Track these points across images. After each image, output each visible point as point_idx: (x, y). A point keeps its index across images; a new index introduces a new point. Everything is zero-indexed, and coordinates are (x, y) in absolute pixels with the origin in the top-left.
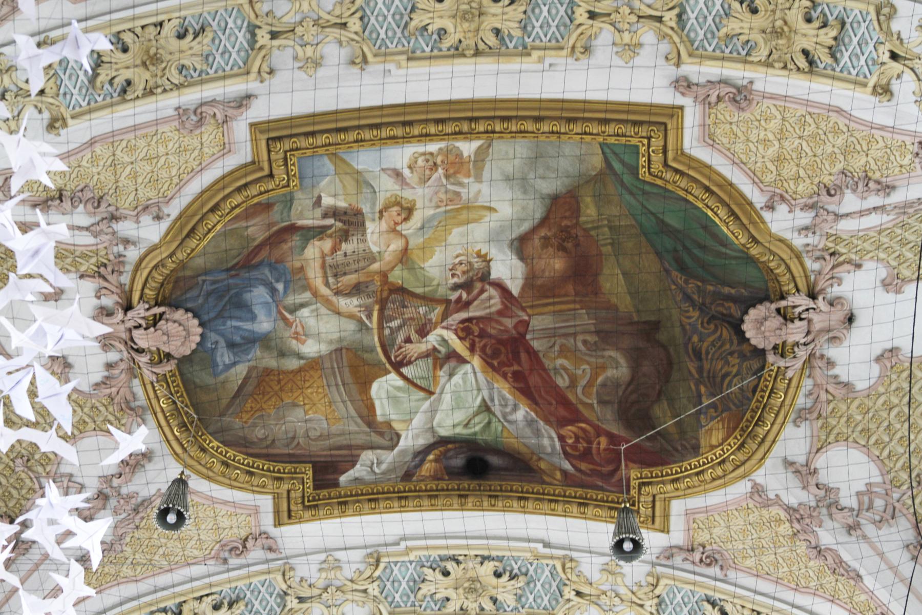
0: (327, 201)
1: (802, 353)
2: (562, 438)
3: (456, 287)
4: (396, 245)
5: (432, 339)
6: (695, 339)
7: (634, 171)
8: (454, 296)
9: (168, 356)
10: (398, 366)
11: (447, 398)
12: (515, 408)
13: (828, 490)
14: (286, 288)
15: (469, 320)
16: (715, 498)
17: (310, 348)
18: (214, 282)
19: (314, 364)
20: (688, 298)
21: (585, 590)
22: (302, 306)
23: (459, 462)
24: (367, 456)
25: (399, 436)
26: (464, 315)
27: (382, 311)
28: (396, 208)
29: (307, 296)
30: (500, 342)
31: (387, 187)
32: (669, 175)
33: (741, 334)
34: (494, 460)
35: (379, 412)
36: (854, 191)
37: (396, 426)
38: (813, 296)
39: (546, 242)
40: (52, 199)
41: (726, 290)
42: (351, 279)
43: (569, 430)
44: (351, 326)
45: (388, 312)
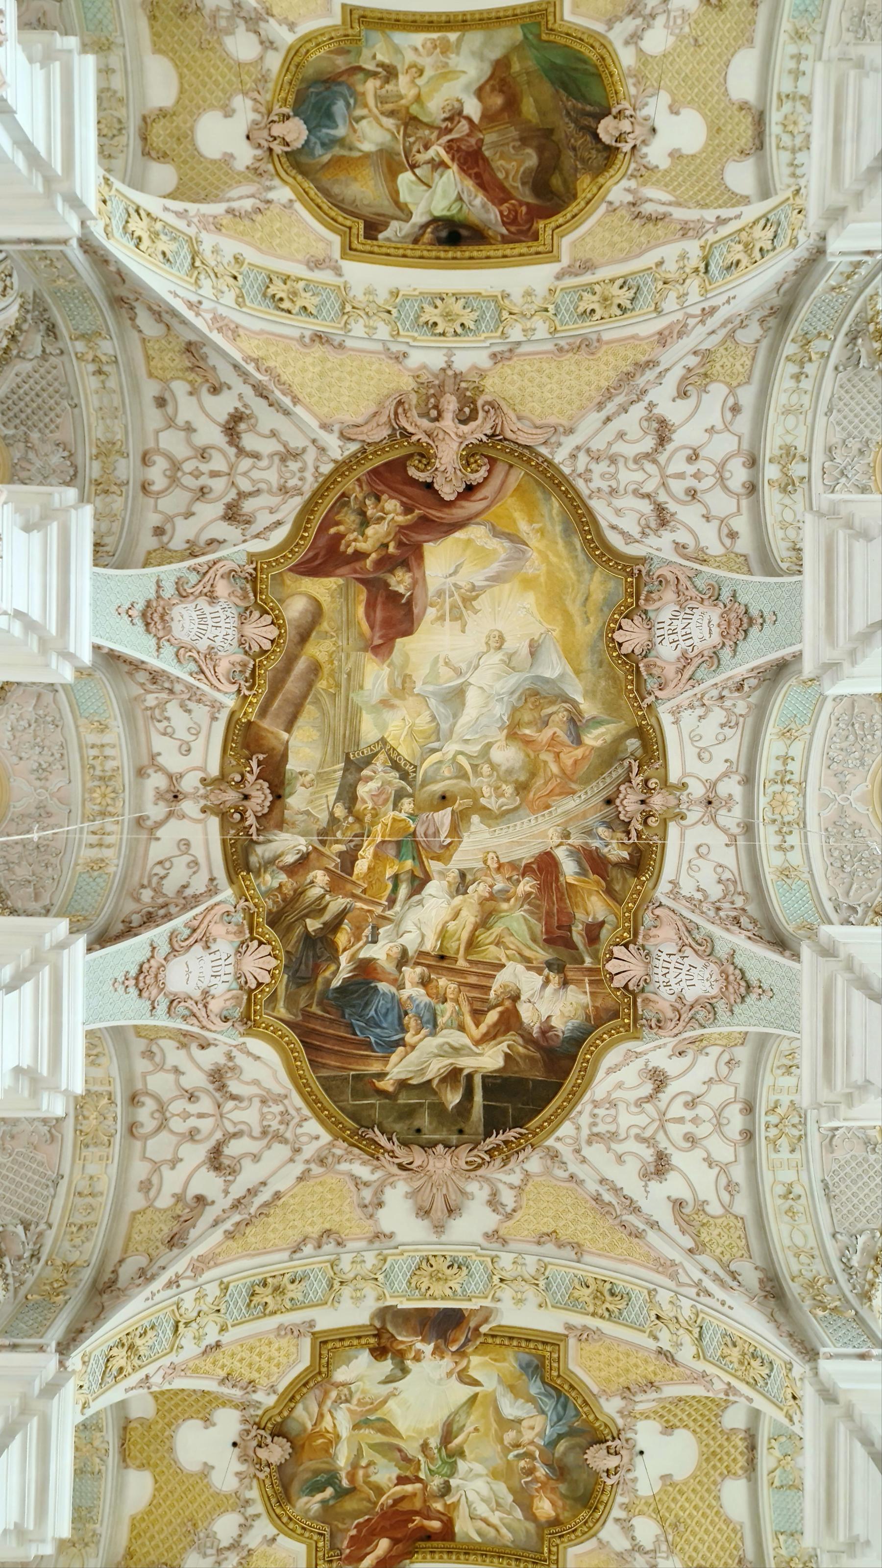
0: (379, 57)
2: (501, 213)
3: (445, 120)
4: (413, 92)
5: (431, 153)
7: (538, 36)
8: (444, 125)
10: (413, 167)
11: (439, 190)
15: (451, 140)
17: (367, 147)
18: (317, 94)
19: (367, 155)
20: (568, 114)
21: (515, 310)
22: (363, 118)
23: (444, 234)
24: (394, 225)
26: (449, 137)
29: (364, 112)
30: (468, 153)
31: (410, 57)
33: (596, 136)
34: (464, 232)
37: (411, 207)
39: (493, 89)
41: (589, 108)
42: (389, 107)
44: (388, 137)
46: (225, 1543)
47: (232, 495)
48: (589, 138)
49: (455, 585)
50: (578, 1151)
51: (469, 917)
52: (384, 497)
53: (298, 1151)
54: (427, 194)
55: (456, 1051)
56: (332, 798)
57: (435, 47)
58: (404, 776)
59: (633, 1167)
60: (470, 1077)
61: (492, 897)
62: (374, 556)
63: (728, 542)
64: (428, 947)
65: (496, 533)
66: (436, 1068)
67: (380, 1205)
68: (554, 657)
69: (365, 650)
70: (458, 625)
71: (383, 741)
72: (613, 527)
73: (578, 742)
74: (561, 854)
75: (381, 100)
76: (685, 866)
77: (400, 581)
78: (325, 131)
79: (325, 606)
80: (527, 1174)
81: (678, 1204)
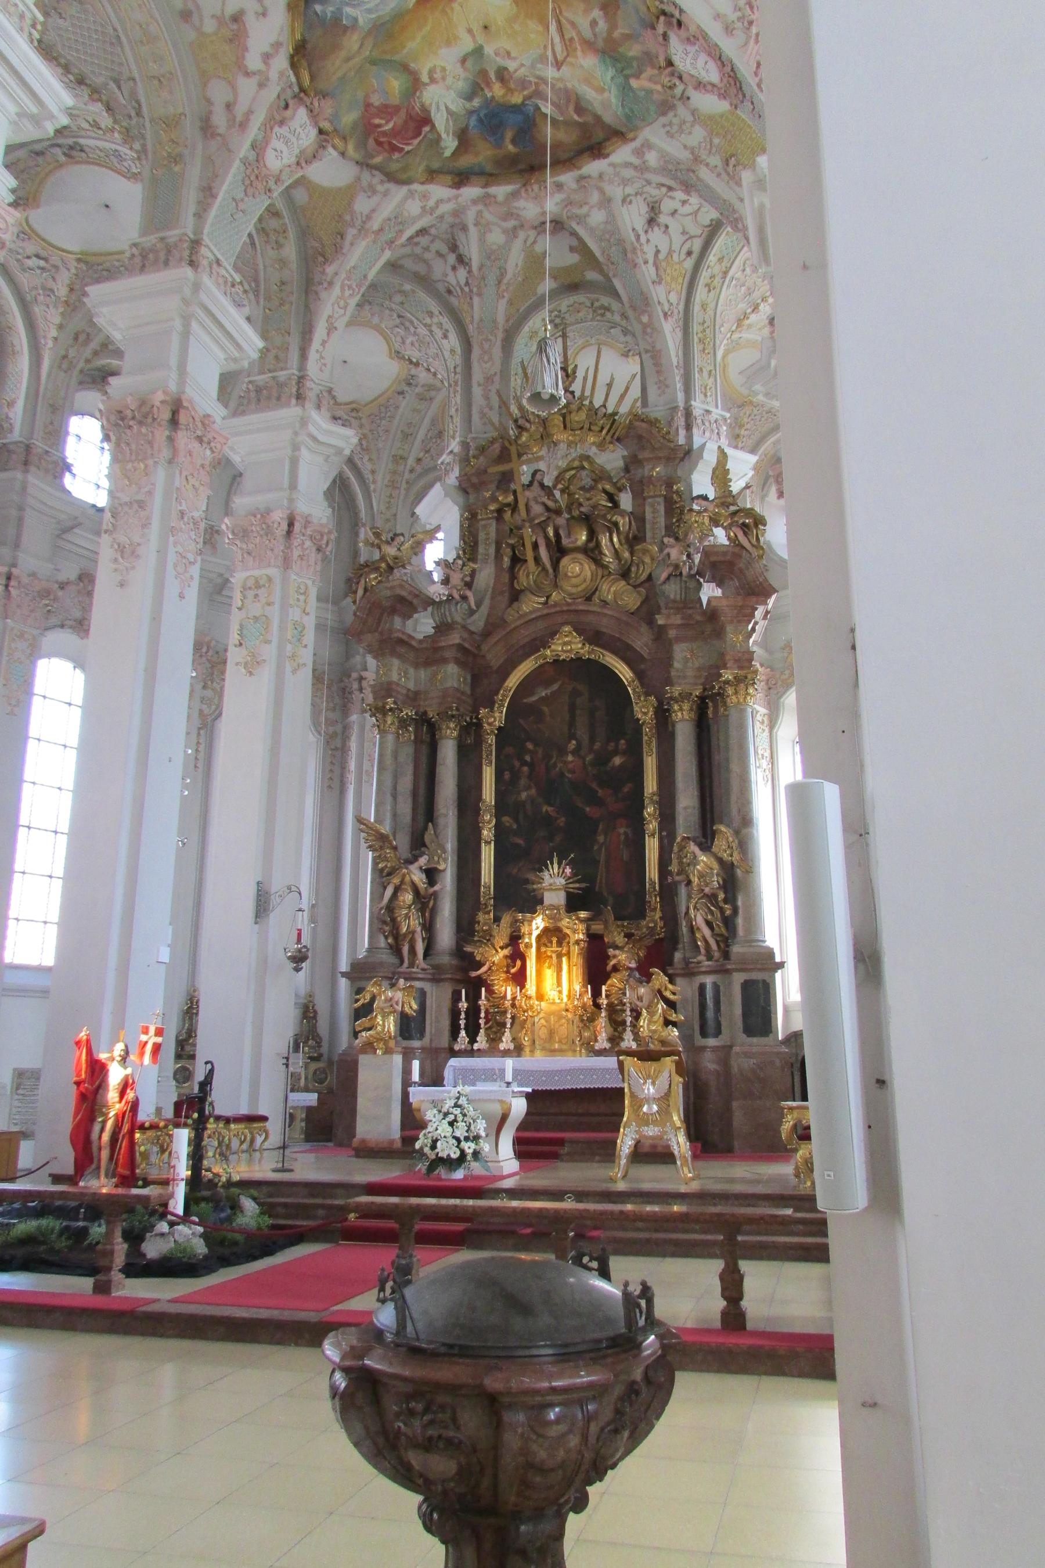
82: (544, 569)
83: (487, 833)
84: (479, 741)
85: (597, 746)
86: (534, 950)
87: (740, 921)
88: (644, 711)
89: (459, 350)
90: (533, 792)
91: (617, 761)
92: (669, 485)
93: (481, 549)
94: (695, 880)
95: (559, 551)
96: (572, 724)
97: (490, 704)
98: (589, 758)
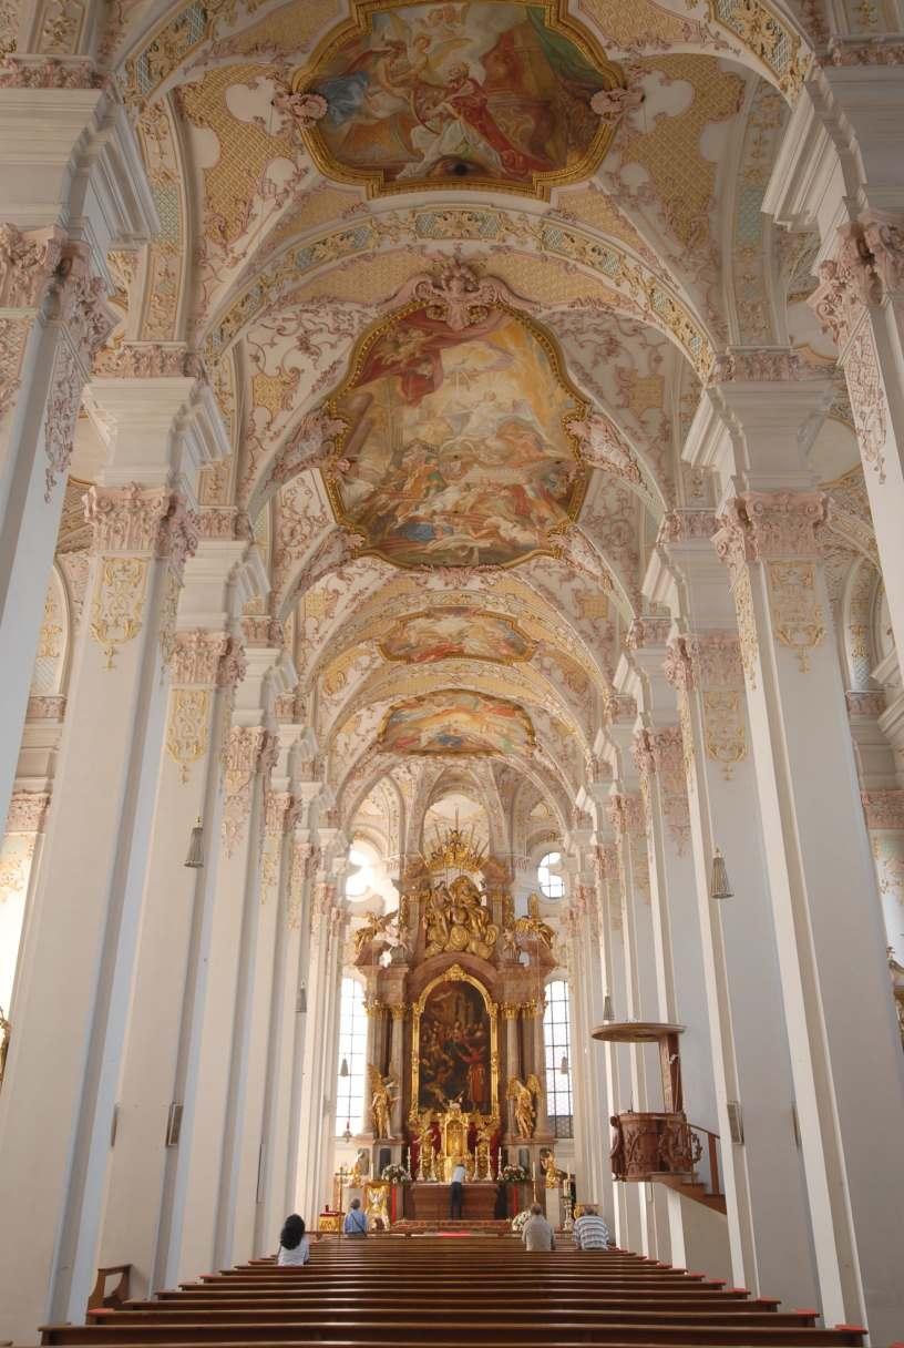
0: (386, 37)
1: (618, 118)
2: (501, 157)
4: (422, 61)
5: (440, 108)
6: (568, 109)
8: (451, 86)
9: (312, 118)
12: (479, 142)
13: (623, 186)
14: (369, 84)
15: (458, 98)
16: (572, 188)
17: (381, 114)
19: (382, 122)
22: (377, 93)
23: (452, 167)
24: (410, 166)
25: (423, 156)
27: (416, 93)
28: (422, 41)
29: (378, 88)
30: (474, 109)
31: (417, 29)
32: (559, 28)
34: (469, 166)
35: (414, 143)
36: (651, 44)
37: (422, 151)
38: (625, 88)
40: (253, 50)
41: (584, 84)
42: (400, 78)
43: (505, 153)
44: (400, 103)
45: (419, 95)
46: (364, 666)
47: (301, 331)
48: (582, 106)
49: (464, 370)
50: (528, 573)
51: (471, 499)
52: (410, 331)
53: (383, 574)
54: (437, 140)
55: (464, 540)
56: (387, 462)
57: (441, 18)
58: (432, 450)
59: (556, 577)
60: (472, 549)
61: (485, 493)
62: (405, 361)
63: (653, 364)
64: (449, 508)
65: (491, 347)
66: (452, 545)
67: (425, 583)
68: (529, 412)
69: (403, 404)
70: (465, 386)
71: (417, 439)
72: (574, 363)
73: (541, 450)
74: (526, 487)
75: (390, 74)
76: (599, 492)
77: (425, 370)
78: (342, 101)
79: (373, 392)
80: (501, 578)
81: (579, 591)
82: (443, 931)
83: (415, 1068)
84: (411, 1020)
85: (469, 1026)
86: (445, 1131)
87: (539, 1121)
88: (491, 1009)
89: (398, 804)
90: (438, 1047)
91: (479, 1034)
92: (504, 896)
93: (411, 917)
94: (519, 1099)
95: (451, 923)
96: (457, 1013)
97: (417, 1001)
98: (465, 1032)
